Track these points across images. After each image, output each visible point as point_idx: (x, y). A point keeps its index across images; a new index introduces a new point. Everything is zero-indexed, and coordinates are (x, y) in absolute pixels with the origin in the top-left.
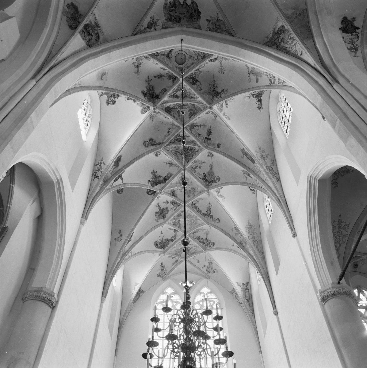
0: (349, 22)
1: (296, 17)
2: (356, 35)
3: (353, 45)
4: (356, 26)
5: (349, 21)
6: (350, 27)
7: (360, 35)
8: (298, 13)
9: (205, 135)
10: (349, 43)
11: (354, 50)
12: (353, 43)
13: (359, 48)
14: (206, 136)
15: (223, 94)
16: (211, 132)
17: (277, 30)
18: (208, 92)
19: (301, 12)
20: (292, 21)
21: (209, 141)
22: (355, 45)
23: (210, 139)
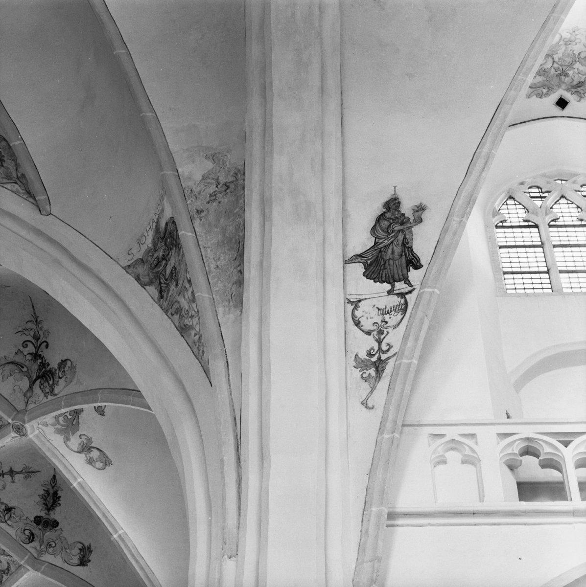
0: (402, 224)
1: (213, 196)
2: (402, 295)
3: (380, 342)
4: (415, 250)
5: (403, 220)
6: (398, 250)
7: (411, 298)
8: (222, 180)
9: (32, 508)
10: (369, 333)
11: (372, 372)
12: (383, 333)
13: (389, 368)
14: (39, 511)
15: (62, 382)
16: (60, 493)
17: (163, 225)
18: (12, 363)
19: (230, 179)
20: (198, 212)
21: (49, 535)
22: (384, 347)
23: (55, 524)
